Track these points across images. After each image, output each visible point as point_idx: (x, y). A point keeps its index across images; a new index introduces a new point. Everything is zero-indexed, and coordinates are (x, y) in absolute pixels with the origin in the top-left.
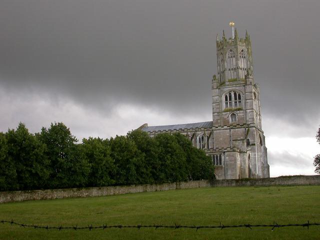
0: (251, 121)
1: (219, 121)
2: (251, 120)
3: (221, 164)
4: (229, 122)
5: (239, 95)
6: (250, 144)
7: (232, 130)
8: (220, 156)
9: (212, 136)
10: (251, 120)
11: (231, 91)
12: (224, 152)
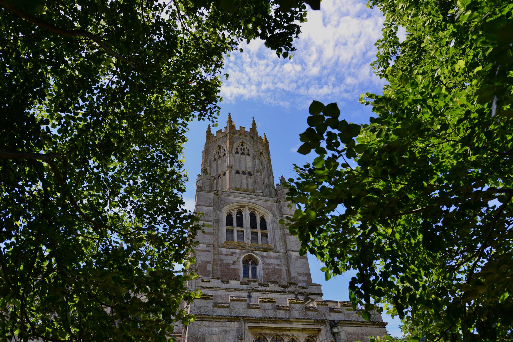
5: (263, 220)
7: (254, 295)
11: (243, 207)
12: (334, 324)
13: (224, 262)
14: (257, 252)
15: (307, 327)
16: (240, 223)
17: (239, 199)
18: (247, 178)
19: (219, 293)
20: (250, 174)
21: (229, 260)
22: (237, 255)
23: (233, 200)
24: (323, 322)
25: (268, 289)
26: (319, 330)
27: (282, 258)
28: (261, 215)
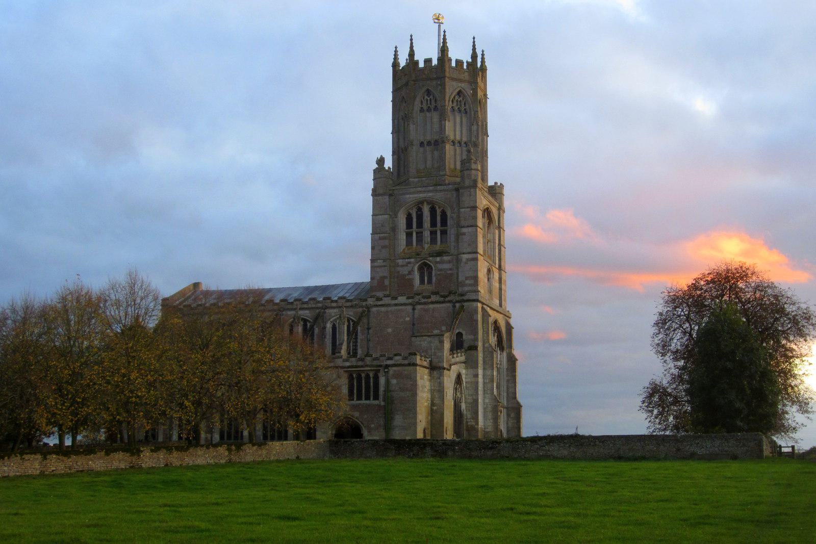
0: (470, 285)
1: (387, 282)
2: (471, 282)
3: (376, 397)
4: (412, 285)
5: (444, 214)
6: (466, 345)
7: (418, 307)
8: (376, 378)
9: (365, 320)
10: (471, 282)
11: (422, 202)
12: (387, 366)
16: (420, 224)
19: (390, 309)
21: (405, 271)
24: (380, 366)
25: (430, 300)
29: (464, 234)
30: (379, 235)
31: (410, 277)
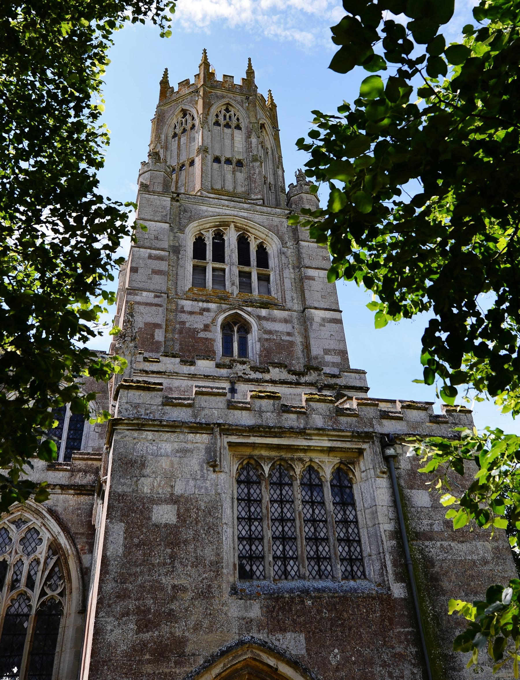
5: (262, 251)
7: (241, 387)
11: (226, 224)
13: (187, 325)
14: (249, 309)
15: (339, 444)
17: (217, 210)
18: (234, 172)
20: (240, 164)
22: (212, 314)
23: (207, 211)
24: (367, 437)
25: (267, 377)
26: (361, 452)
27: (295, 321)
28: (258, 242)
29: (312, 278)
30: (149, 251)
31: (209, 335)
